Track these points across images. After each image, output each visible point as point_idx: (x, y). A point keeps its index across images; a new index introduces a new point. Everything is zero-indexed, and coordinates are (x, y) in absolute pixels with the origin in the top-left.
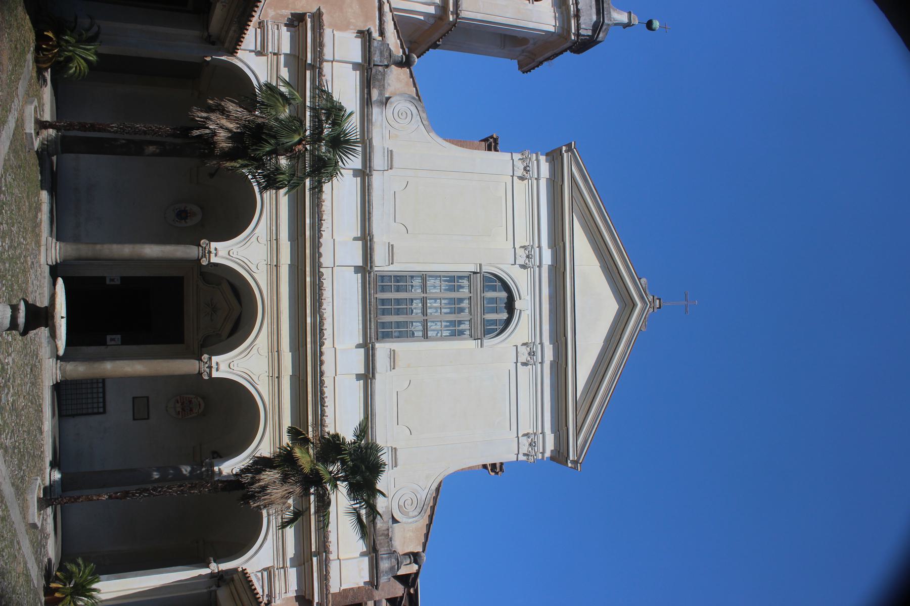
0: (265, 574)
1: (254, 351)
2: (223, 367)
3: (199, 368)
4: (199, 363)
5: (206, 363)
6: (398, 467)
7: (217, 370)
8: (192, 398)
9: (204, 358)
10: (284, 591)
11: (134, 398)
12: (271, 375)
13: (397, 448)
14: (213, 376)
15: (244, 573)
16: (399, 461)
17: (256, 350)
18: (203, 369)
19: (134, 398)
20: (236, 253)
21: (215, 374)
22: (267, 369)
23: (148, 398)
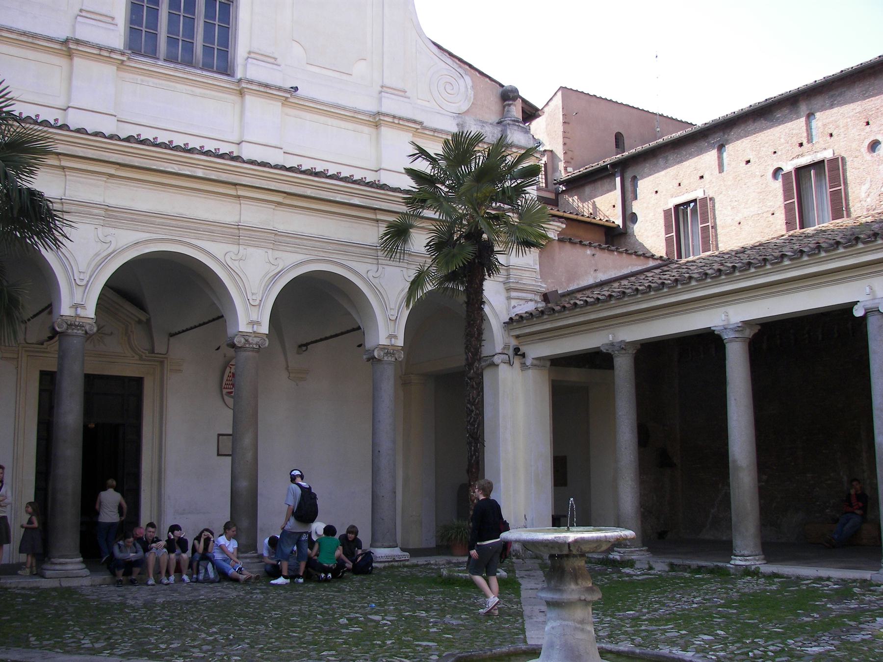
0: (514, 294)
1: (234, 265)
2: (254, 318)
3: (253, 351)
4: (245, 351)
5: (247, 340)
6: (406, 89)
7: (258, 323)
8: (230, 372)
9: (239, 342)
10: (534, 275)
11: (218, 455)
12: (271, 246)
13: (380, 84)
14: (268, 333)
15: (511, 323)
16: (400, 86)
17: (236, 263)
18: (254, 346)
19: (218, 455)
20: (82, 274)
21: (265, 329)
22: (261, 252)
23: (219, 435)
